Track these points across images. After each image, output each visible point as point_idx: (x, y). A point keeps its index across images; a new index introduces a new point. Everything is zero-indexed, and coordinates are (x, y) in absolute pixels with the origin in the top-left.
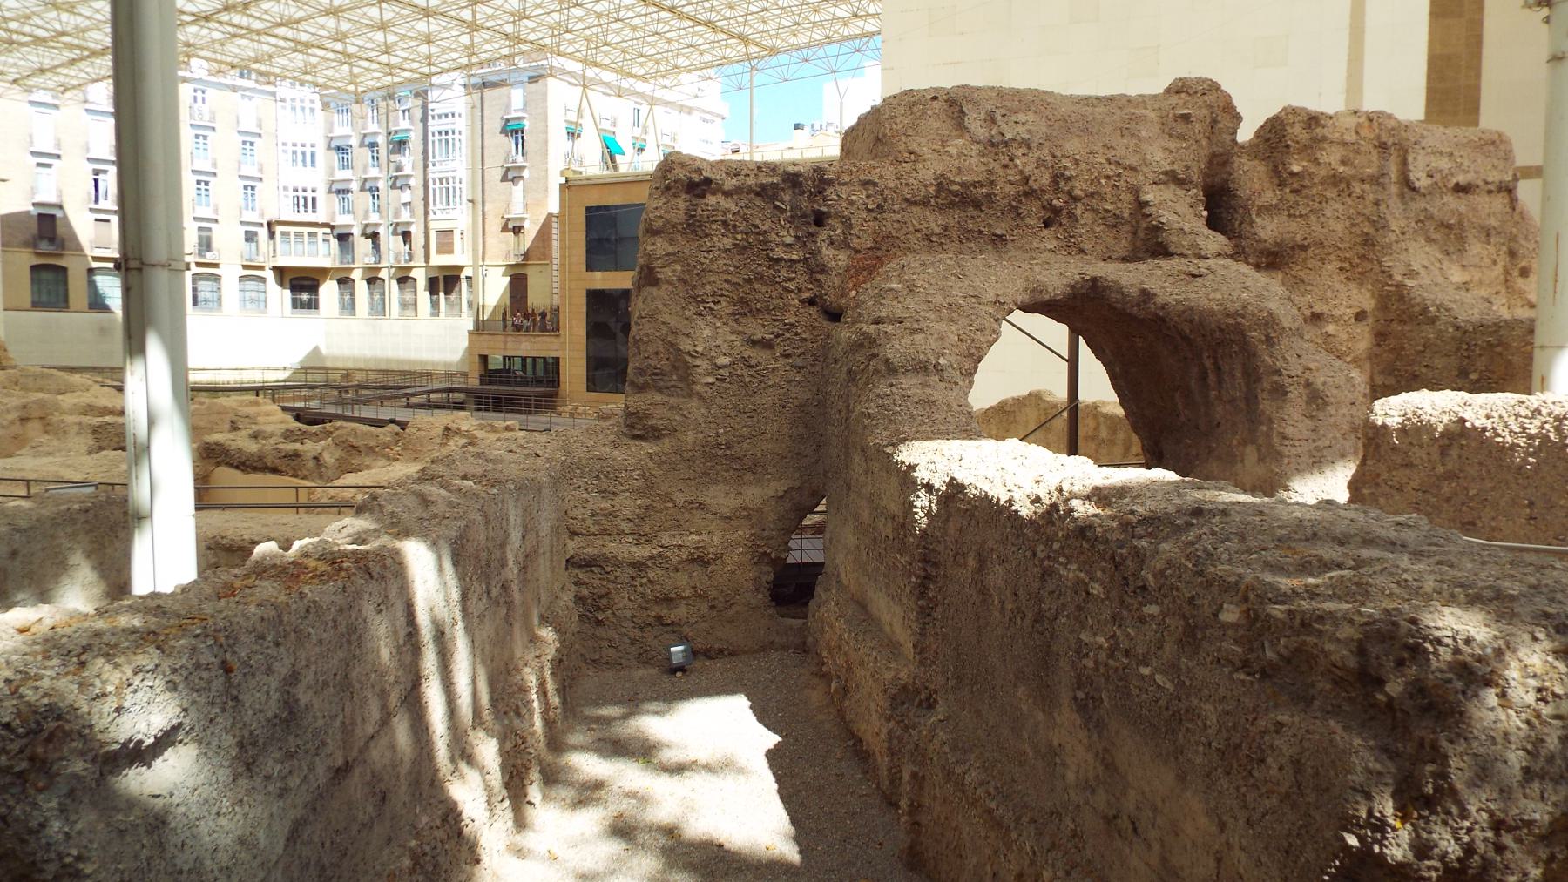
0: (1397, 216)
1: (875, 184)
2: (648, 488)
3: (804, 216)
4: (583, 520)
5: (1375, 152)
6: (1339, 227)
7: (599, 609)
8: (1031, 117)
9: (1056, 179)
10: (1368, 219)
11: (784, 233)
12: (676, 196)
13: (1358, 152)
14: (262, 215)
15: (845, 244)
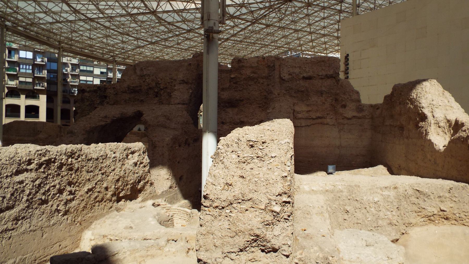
9: (156, 83)
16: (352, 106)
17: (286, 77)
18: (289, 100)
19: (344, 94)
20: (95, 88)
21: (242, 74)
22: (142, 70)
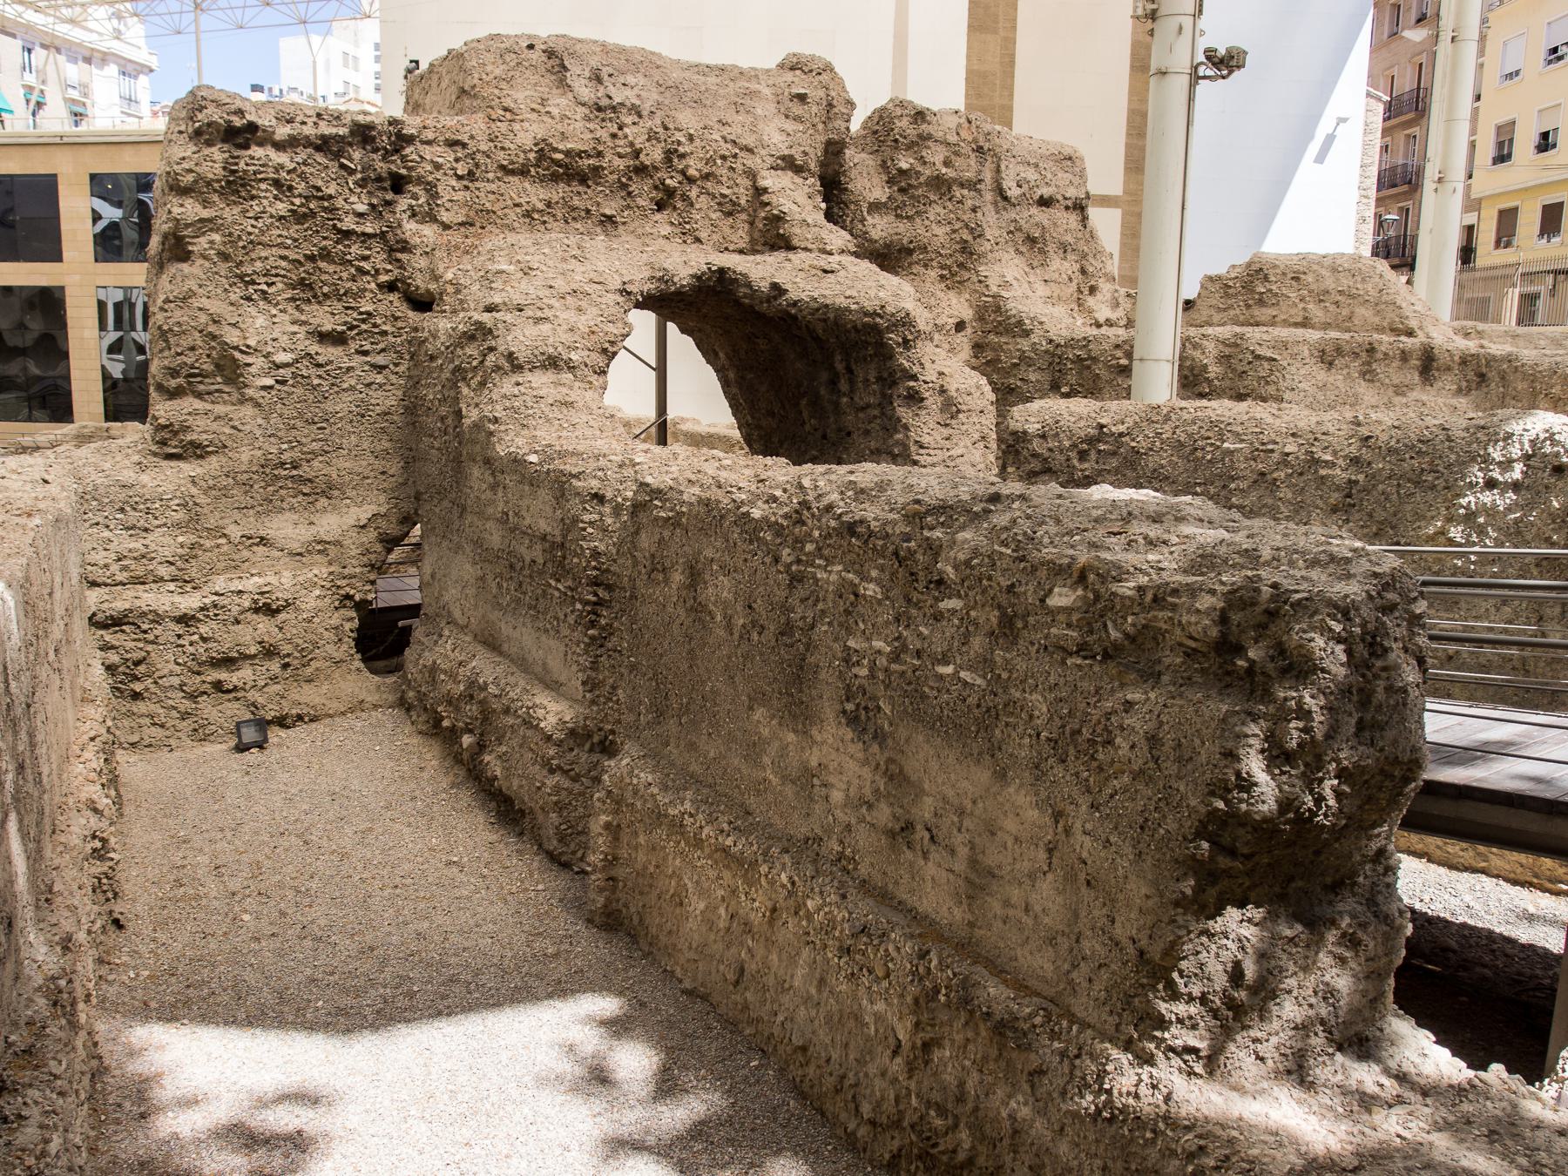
0: (993, 223)
1: (464, 146)
2: (193, 519)
3: (379, 179)
4: (106, 566)
5: (973, 156)
7: (136, 678)
9: (669, 155)
10: (967, 226)
11: (353, 199)
12: (209, 144)
13: (957, 154)
15: (431, 217)
17: (1013, 192)
20: (326, 129)
21: (925, 163)
22: (599, 80)
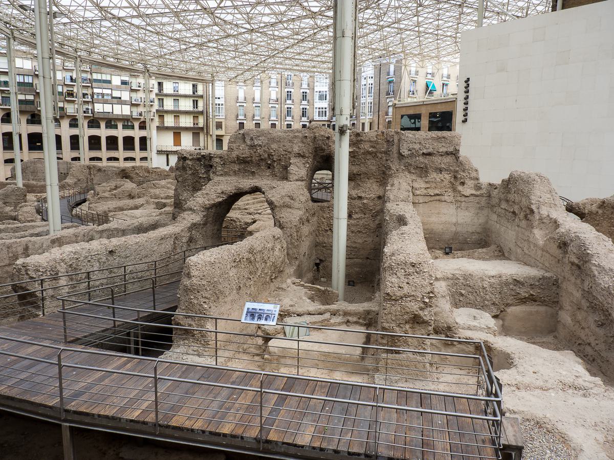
6: (374, 168)
8: (263, 138)
9: (268, 155)
12: (180, 160)
14: (308, 119)
16: (470, 183)
17: (405, 152)
18: (408, 176)
19: (464, 171)
20: (198, 156)
